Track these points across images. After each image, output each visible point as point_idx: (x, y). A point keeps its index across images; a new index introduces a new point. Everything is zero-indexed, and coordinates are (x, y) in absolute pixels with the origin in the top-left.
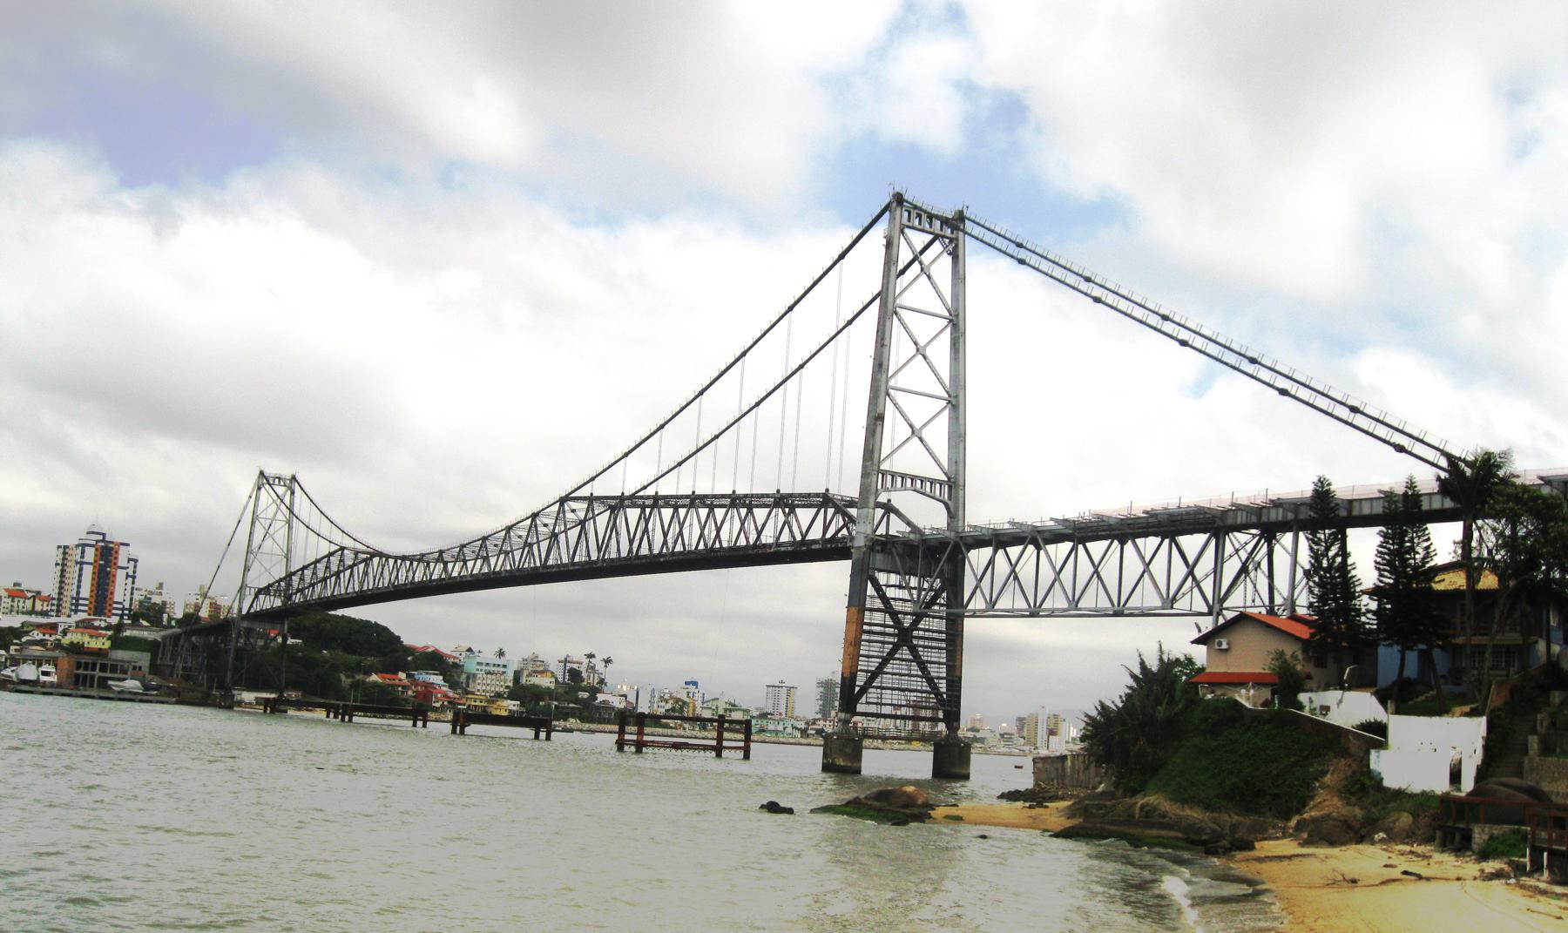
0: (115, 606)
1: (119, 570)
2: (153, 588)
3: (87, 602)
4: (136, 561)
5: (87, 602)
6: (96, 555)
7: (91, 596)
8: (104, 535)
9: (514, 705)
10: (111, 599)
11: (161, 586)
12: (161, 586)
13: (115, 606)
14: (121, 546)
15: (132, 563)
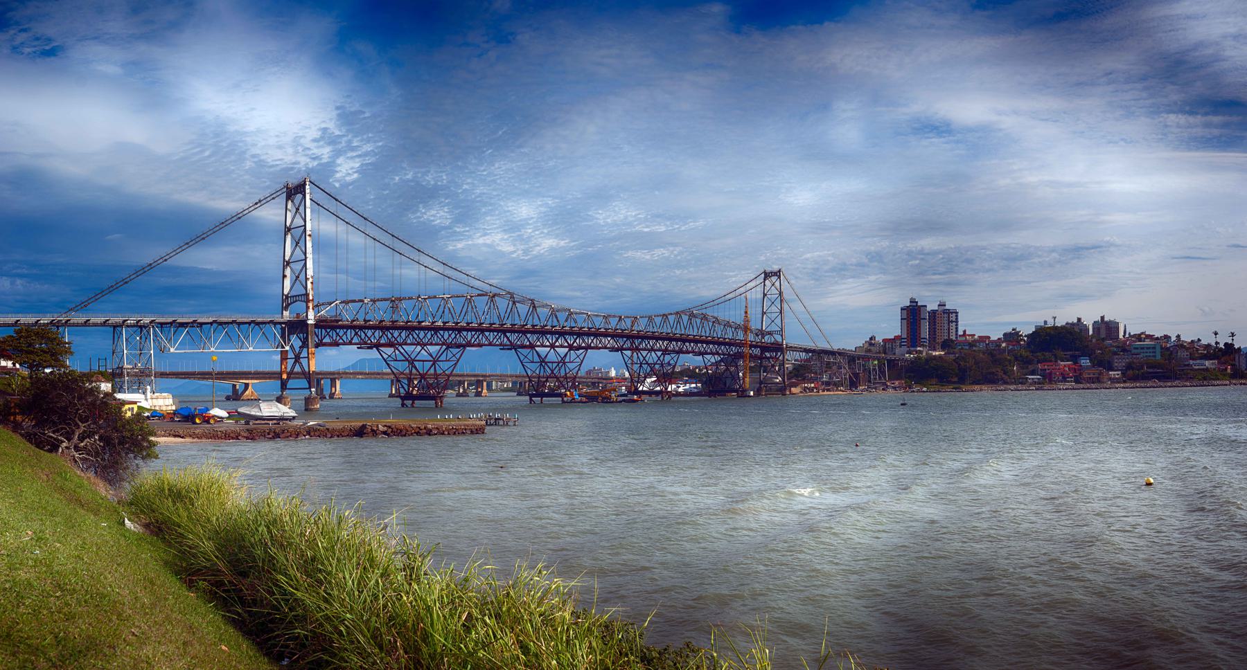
0: (922, 340)
1: (922, 321)
2: (1075, 321)
3: (905, 340)
4: (957, 313)
5: (905, 340)
6: (908, 314)
7: (908, 337)
8: (917, 302)
9: (1118, 375)
10: (920, 337)
11: (1079, 320)
12: (1079, 320)
13: (922, 340)
14: (922, 308)
15: (954, 315)
